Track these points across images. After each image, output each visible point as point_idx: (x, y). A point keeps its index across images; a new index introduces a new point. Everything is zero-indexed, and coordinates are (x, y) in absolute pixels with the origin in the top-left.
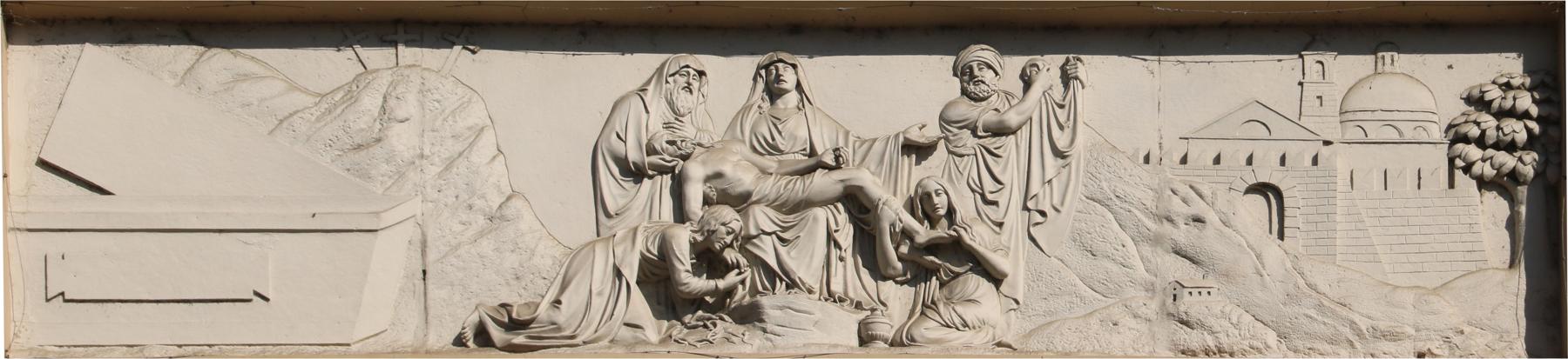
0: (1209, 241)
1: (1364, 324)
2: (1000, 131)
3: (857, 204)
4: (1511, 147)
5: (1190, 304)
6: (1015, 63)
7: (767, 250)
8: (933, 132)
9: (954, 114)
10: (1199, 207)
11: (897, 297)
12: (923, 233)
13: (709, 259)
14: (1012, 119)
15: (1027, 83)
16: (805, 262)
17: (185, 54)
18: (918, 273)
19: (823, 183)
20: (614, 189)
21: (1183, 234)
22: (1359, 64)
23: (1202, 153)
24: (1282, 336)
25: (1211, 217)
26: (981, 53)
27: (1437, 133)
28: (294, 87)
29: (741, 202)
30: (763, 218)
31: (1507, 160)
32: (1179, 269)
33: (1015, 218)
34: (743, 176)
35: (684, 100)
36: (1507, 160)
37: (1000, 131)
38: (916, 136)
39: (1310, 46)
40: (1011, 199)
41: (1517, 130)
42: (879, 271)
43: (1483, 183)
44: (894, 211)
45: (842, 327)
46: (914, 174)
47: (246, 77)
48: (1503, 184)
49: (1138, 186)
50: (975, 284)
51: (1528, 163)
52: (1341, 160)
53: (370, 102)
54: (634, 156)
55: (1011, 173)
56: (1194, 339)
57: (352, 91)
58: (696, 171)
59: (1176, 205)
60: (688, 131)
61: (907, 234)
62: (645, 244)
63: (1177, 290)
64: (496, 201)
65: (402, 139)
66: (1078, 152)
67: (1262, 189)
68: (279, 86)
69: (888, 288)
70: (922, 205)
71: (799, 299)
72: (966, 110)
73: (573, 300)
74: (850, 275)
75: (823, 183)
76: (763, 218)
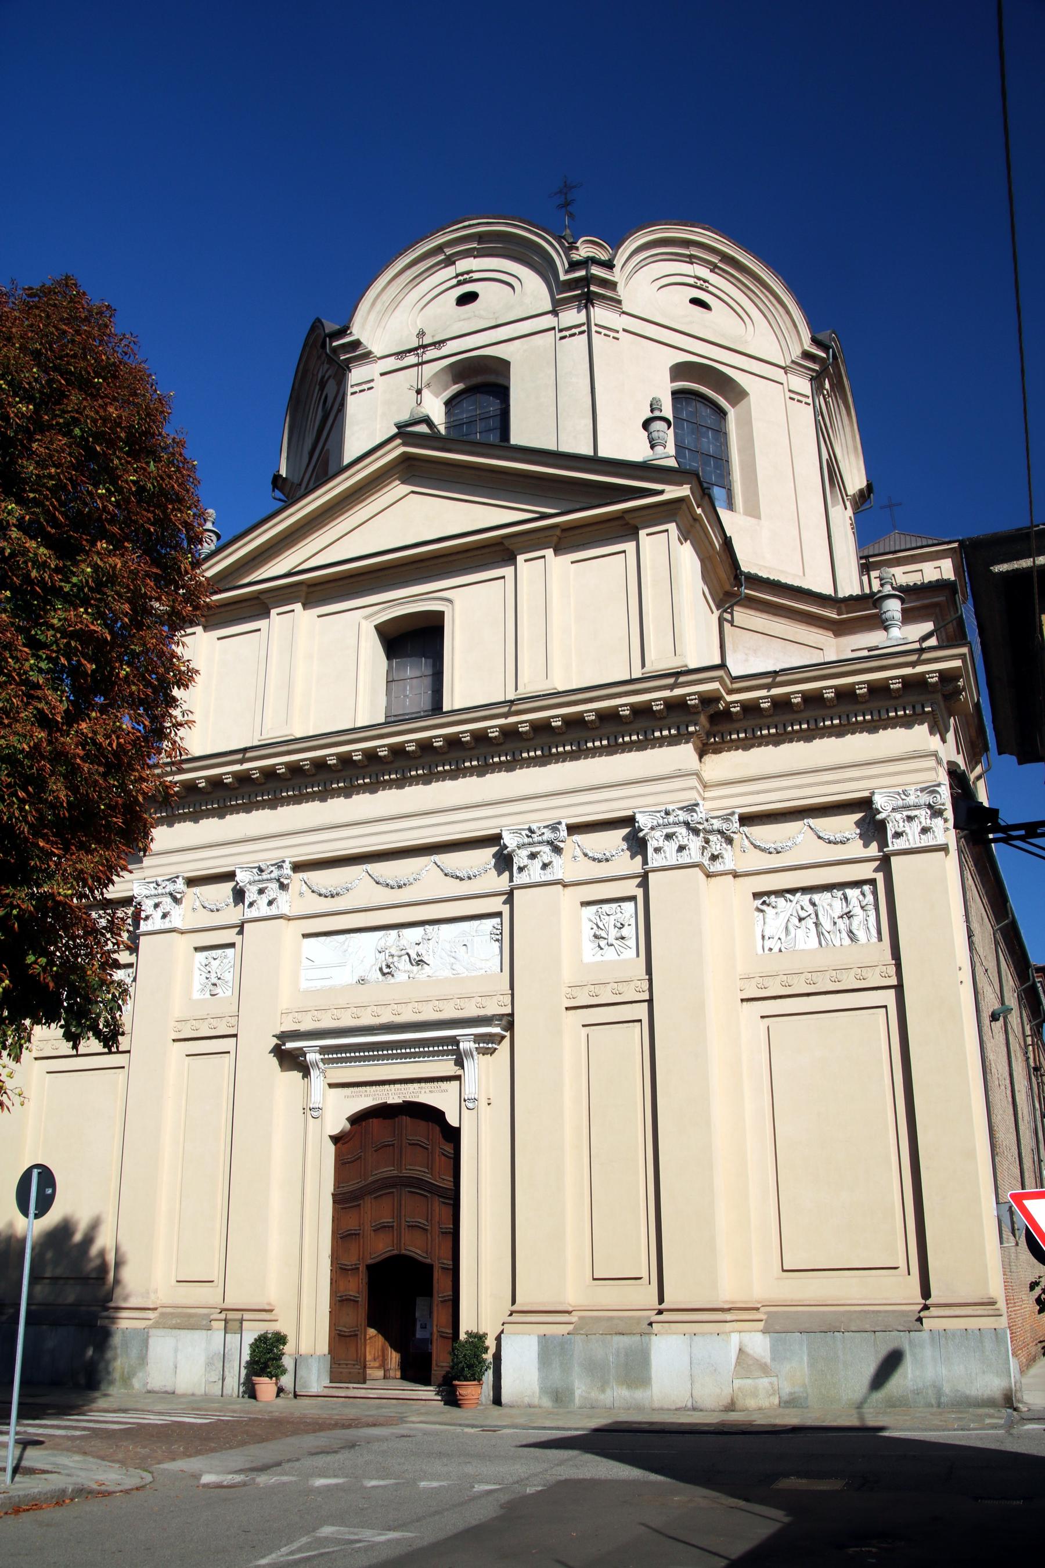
3: (408, 954)
5: (454, 967)
7: (396, 964)
11: (415, 968)
12: (419, 958)
13: (388, 966)
16: (401, 966)
17: (324, 938)
18: (419, 965)
19: (403, 952)
22: (478, 922)
26: (427, 927)
29: (393, 956)
30: (396, 959)
31: (497, 937)
32: (453, 960)
34: (394, 951)
36: (497, 937)
40: (431, 951)
41: (498, 932)
44: (413, 956)
48: (497, 940)
53: (346, 943)
56: (454, 972)
57: (344, 942)
60: (387, 944)
62: (379, 965)
63: (452, 964)
70: (418, 955)
71: (399, 973)
74: (409, 966)
75: (403, 952)
76: (396, 959)
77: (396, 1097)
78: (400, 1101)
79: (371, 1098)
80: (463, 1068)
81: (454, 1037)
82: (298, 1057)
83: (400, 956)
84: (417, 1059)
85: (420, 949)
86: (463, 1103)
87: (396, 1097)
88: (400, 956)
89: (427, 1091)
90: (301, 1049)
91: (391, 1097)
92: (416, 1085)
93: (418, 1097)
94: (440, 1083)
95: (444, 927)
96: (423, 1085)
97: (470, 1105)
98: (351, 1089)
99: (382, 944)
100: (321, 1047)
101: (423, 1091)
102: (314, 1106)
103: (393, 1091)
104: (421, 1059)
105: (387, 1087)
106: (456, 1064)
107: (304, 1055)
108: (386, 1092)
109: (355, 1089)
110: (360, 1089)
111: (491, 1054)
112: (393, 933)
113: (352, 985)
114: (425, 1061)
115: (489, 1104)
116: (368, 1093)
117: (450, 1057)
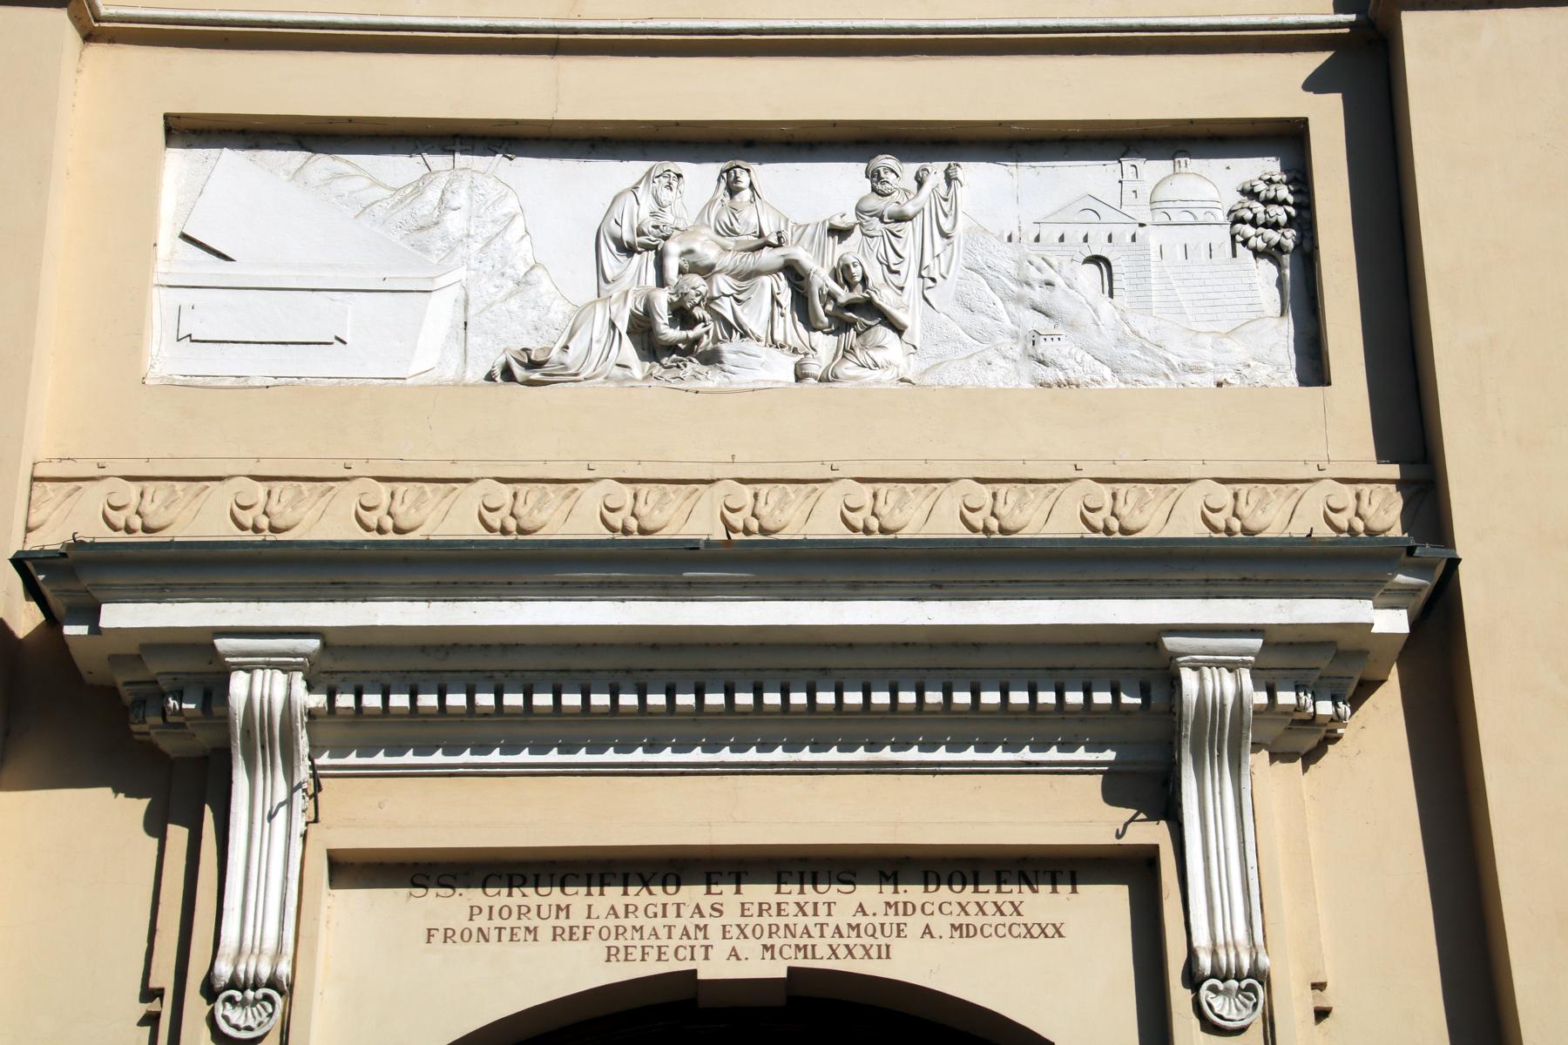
0: (1058, 300)
1: (1175, 361)
2: (900, 218)
3: (794, 273)
4: (1276, 226)
5: (1045, 348)
6: (911, 168)
7: (726, 308)
8: (851, 219)
9: (867, 206)
10: (1050, 274)
11: (825, 344)
12: (844, 295)
13: (682, 315)
14: (910, 209)
15: (920, 183)
16: (754, 317)
17: (296, 157)
18: (840, 325)
19: (769, 257)
20: (611, 261)
21: (1038, 295)
23: (1051, 234)
24: (1115, 371)
25: (1058, 281)
26: (885, 161)
27: (1221, 216)
28: (376, 183)
29: (707, 271)
30: (723, 283)
31: (1274, 236)
32: (1036, 321)
33: (912, 284)
34: (708, 251)
35: (665, 195)
36: (1274, 236)
37: (900, 218)
38: (838, 222)
39: (1126, 154)
40: (909, 269)
42: (811, 326)
43: (1257, 253)
44: (821, 278)
45: (783, 368)
46: (838, 251)
47: (341, 175)
48: (1271, 253)
49: (1004, 259)
50: (883, 334)
51: (1289, 238)
52: (1153, 238)
53: (432, 195)
54: (627, 237)
55: (909, 248)
56: (1049, 374)
57: (418, 188)
58: (674, 248)
59: (1033, 273)
60: (669, 218)
61: (831, 296)
62: (634, 304)
63: (1036, 335)
64: (522, 269)
65: (454, 223)
66: (959, 233)
67: (1096, 260)
68: (364, 182)
69: (818, 337)
70: (843, 274)
71: (749, 345)
72: (875, 203)
73: (578, 346)
74: (789, 328)
75: (769, 257)
76: (723, 283)
77: (750, 948)
78: (777, 970)
79: (594, 948)
80: (1168, 809)
81: (1150, 638)
82: (152, 696)
83: (750, 275)
84: (886, 754)
85: (850, 250)
86: (1180, 997)
87: (750, 948)
88: (750, 275)
89: (940, 924)
90: (200, 643)
91: (721, 948)
92: (871, 895)
93: (885, 953)
94: (1015, 893)
95: (977, 176)
96: (913, 893)
97: (1223, 1007)
98: (474, 895)
99: (637, 214)
100: (333, 642)
101: (915, 923)
102: (247, 968)
103: (732, 916)
104: (913, 754)
105: (693, 893)
106: (1113, 795)
107: (214, 689)
108: (688, 920)
109: (498, 897)
110: (527, 896)
111: (1310, 757)
112: (701, 177)
113: (459, 385)
114: (935, 769)
115: (1321, 1014)
116: (578, 918)
117: (1081, 754)
